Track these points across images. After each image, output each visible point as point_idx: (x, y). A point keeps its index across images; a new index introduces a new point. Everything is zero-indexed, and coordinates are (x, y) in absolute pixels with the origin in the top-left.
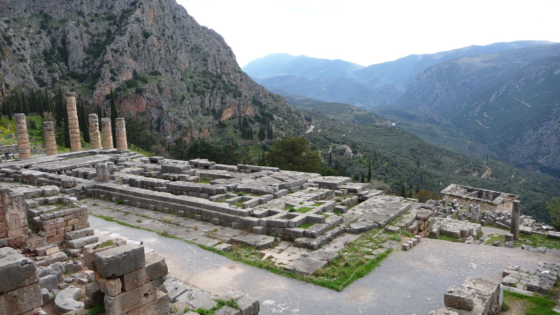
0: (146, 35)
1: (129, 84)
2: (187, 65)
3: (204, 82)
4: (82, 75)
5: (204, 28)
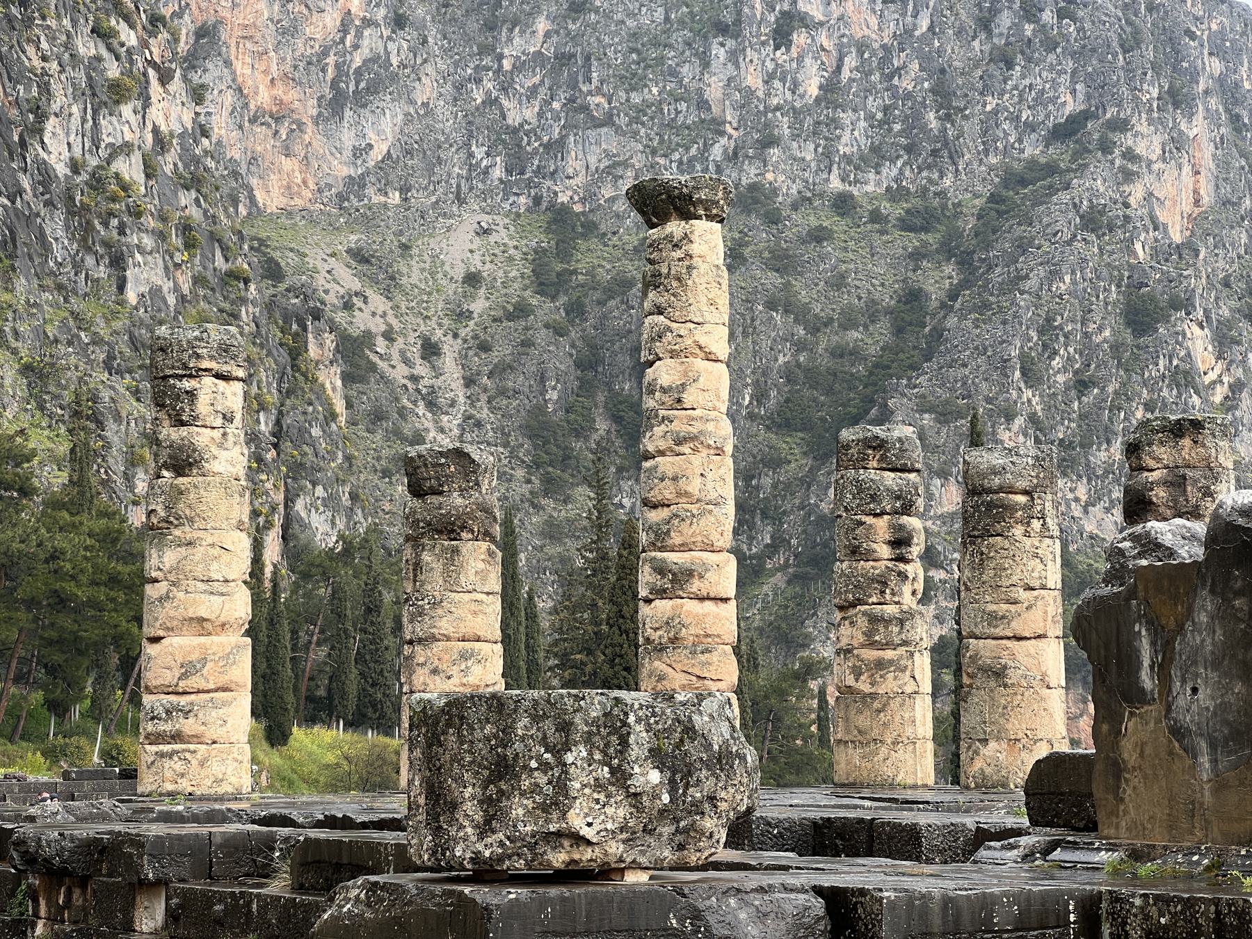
0: (1144, 314)
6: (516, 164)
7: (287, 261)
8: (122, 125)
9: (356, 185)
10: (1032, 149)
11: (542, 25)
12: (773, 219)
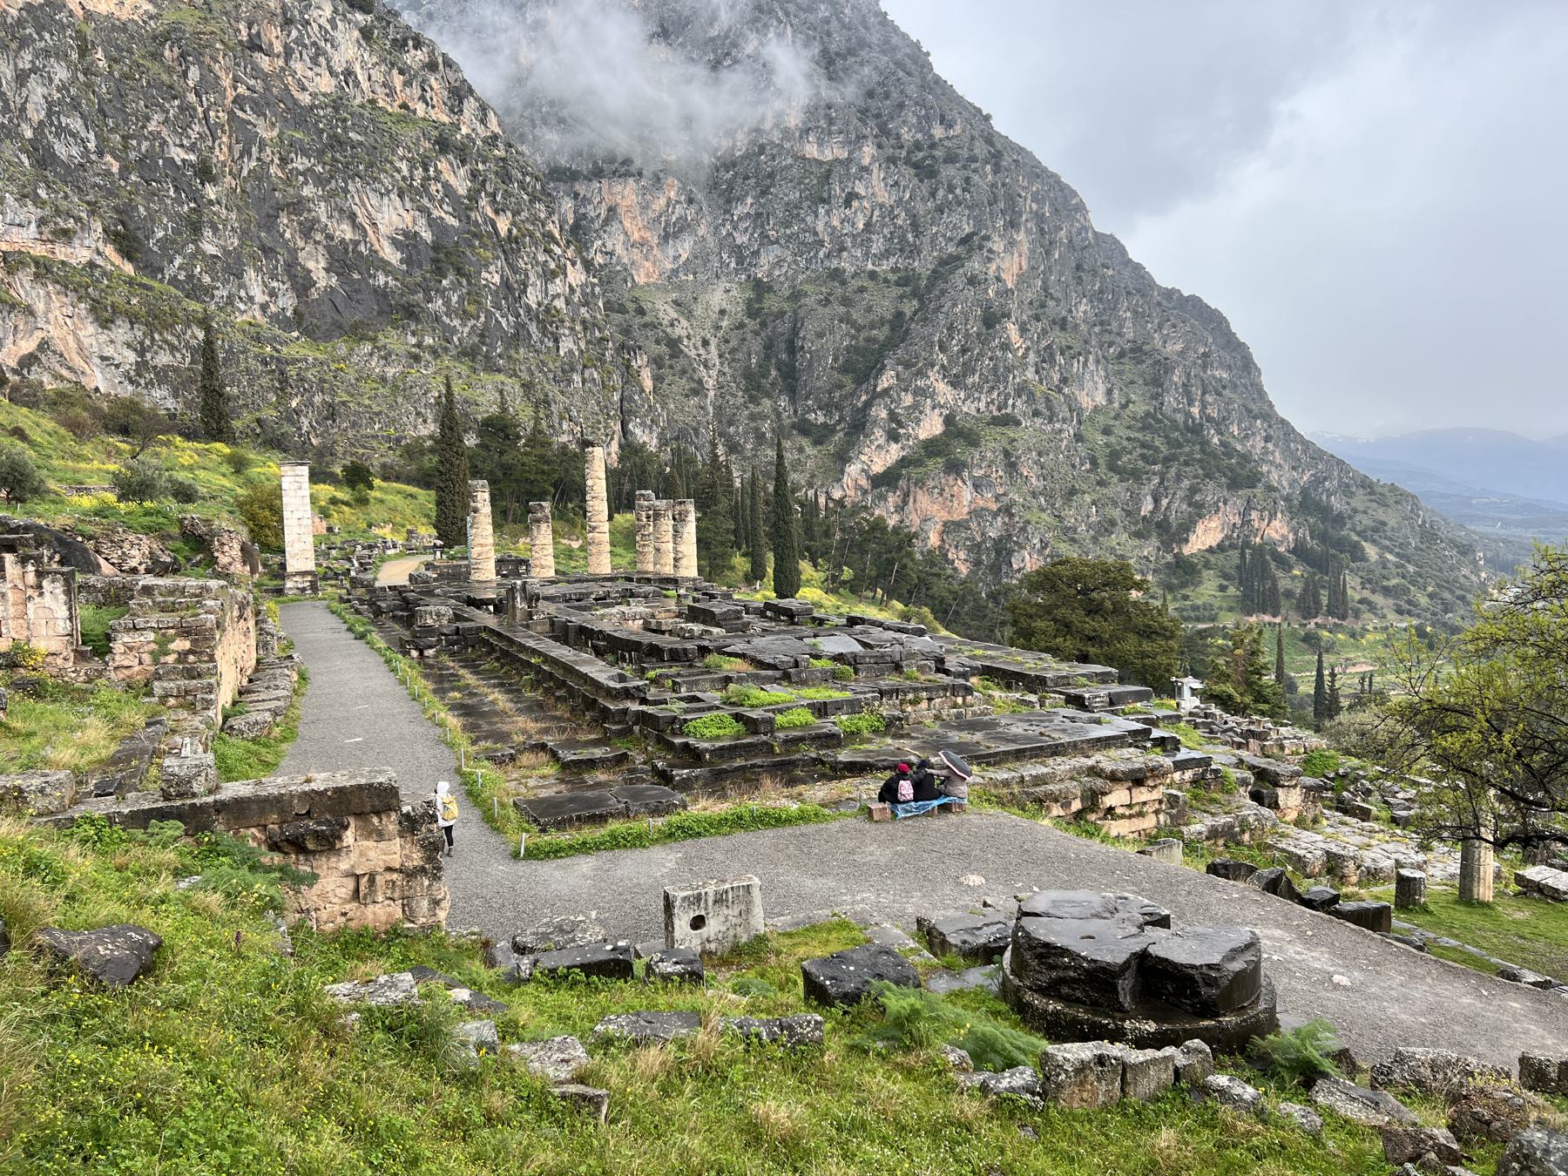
0: (991, 320)
1: (932, 447)
2: (1100, 399)
3: (1144, 445)
4: (825, 425)
5: (1170, 294)
6: (740, 262)
7: (647, 306)
8: (557, 286)
9: (675, 272)
10: (951, 249)
11: (749, 200)
12: (843, 283)
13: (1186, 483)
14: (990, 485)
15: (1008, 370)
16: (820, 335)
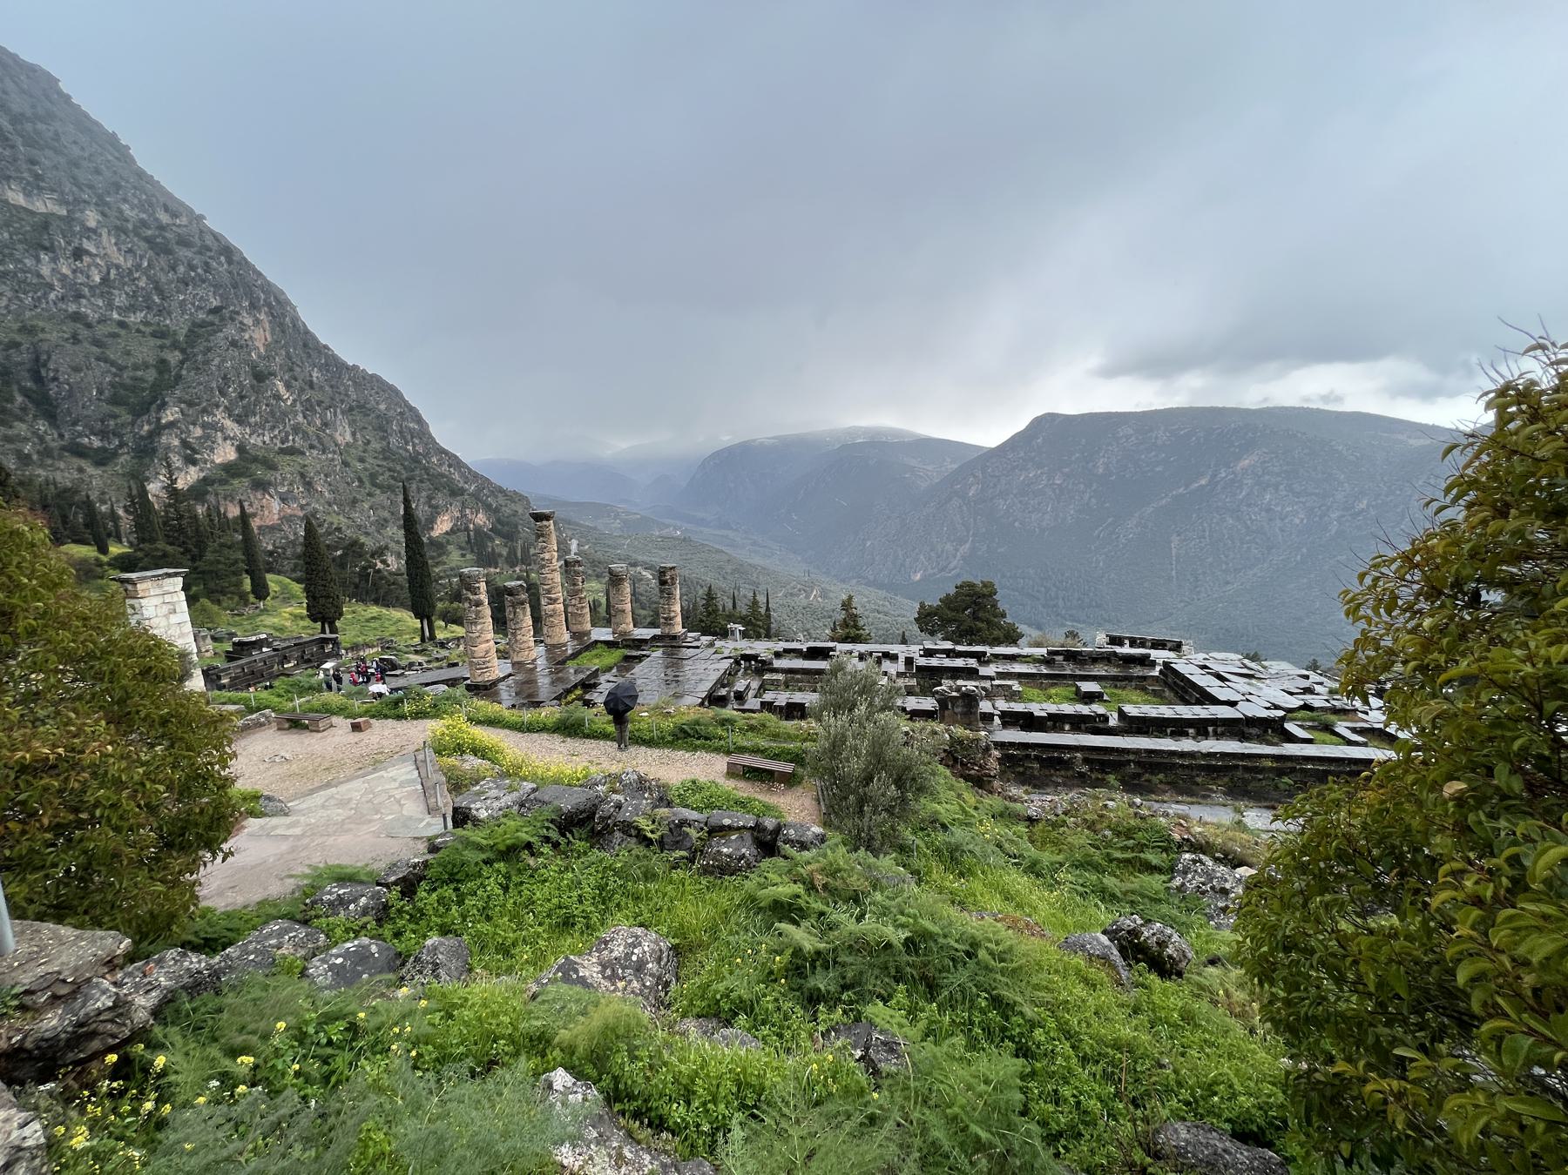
0: (260, 377)
1: (230, 470)
3: (390, 470)
4: (104, 449)
13: (424, 494)
14: (295, 499)
15: (285, 414)
16: (77, 369)
